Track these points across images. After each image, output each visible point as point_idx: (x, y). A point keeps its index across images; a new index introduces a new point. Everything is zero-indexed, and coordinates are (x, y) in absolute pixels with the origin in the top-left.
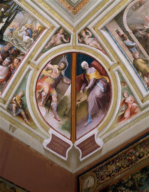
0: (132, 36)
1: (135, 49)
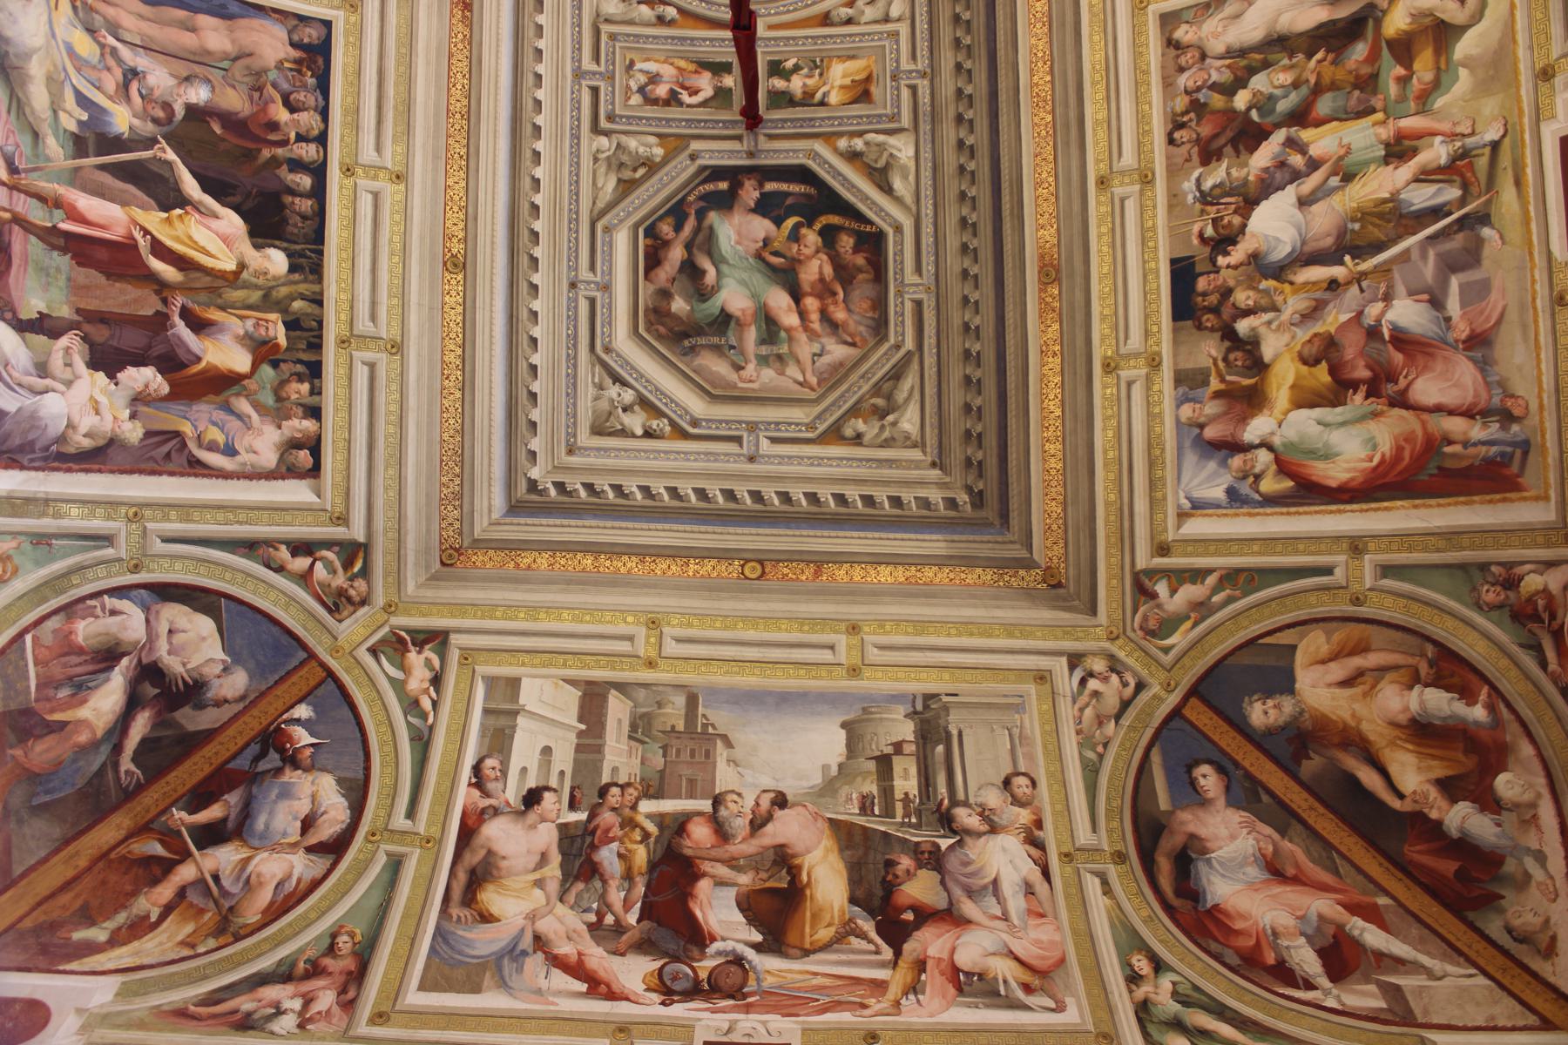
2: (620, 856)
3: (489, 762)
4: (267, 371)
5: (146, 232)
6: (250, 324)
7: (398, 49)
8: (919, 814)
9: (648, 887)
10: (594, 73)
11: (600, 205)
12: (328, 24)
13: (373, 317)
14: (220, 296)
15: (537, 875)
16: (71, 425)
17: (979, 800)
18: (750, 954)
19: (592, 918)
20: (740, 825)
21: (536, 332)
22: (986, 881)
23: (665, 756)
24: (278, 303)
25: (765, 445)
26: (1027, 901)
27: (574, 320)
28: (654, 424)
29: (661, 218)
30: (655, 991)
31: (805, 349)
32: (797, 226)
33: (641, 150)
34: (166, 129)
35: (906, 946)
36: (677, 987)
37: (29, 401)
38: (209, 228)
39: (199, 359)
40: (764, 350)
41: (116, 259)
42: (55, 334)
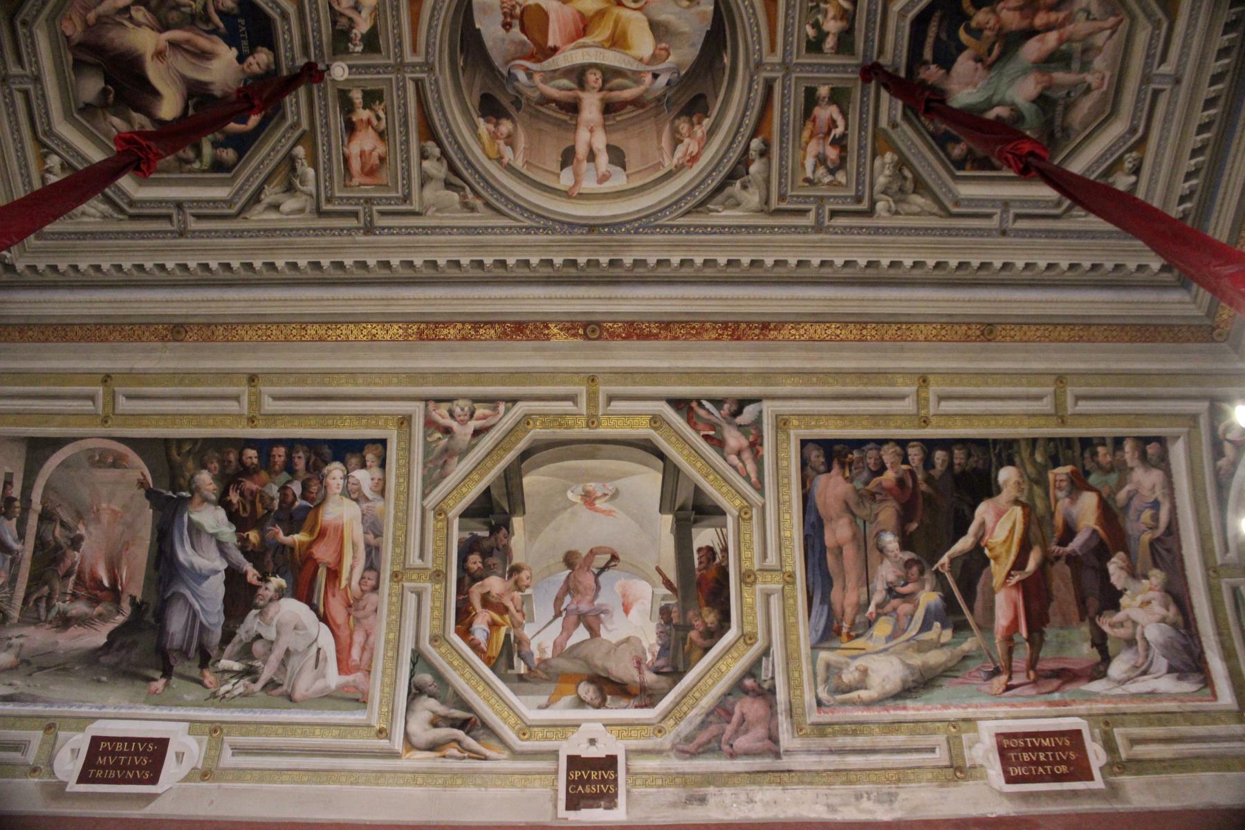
0: (33, 521)
1: (8, 563)
4: (1093, 479)
5: (1009, 575)
6: (1060, 494)
7: (813, 384)
10: (818, 214)
11: (935, 209)
12: (804, 443)
13: (1038, 398)
14: (1043, 517)
16: (1163, 620)
21: (1042, 264)
24: (1040, 473)
25: (1166, 69)
27: (1032, 233)
28: (1128, 165)
29: (948, 155)
31: (1080, 27)
32: (969, 30)
33: (887, 172)
34: (925, 564)
37: (1156, 652)
38: (994, 528)
39: (1094, 531)
40: (1076, 65)
41: (1035, 594)
42: (1104, 636)
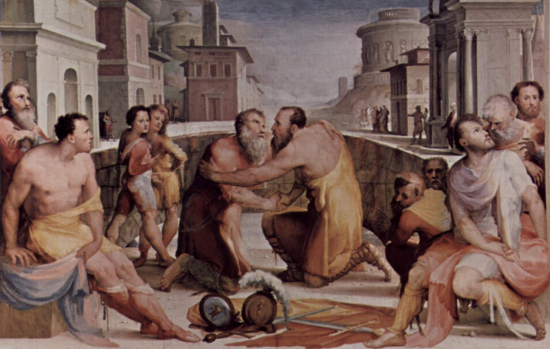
2: (154, 185)
3: (17, 90)
8: (429, 129)
9: (182, 217)
15: (80, 211)
17: (487, 113)
18: (276, 283)
19: (136, 253)
20: (262, 146)
22: (488, 199)
23: (186, 74)
26: (522, 221)
30: (198, 326)
35: (412, 273)
36: (217, 321)
